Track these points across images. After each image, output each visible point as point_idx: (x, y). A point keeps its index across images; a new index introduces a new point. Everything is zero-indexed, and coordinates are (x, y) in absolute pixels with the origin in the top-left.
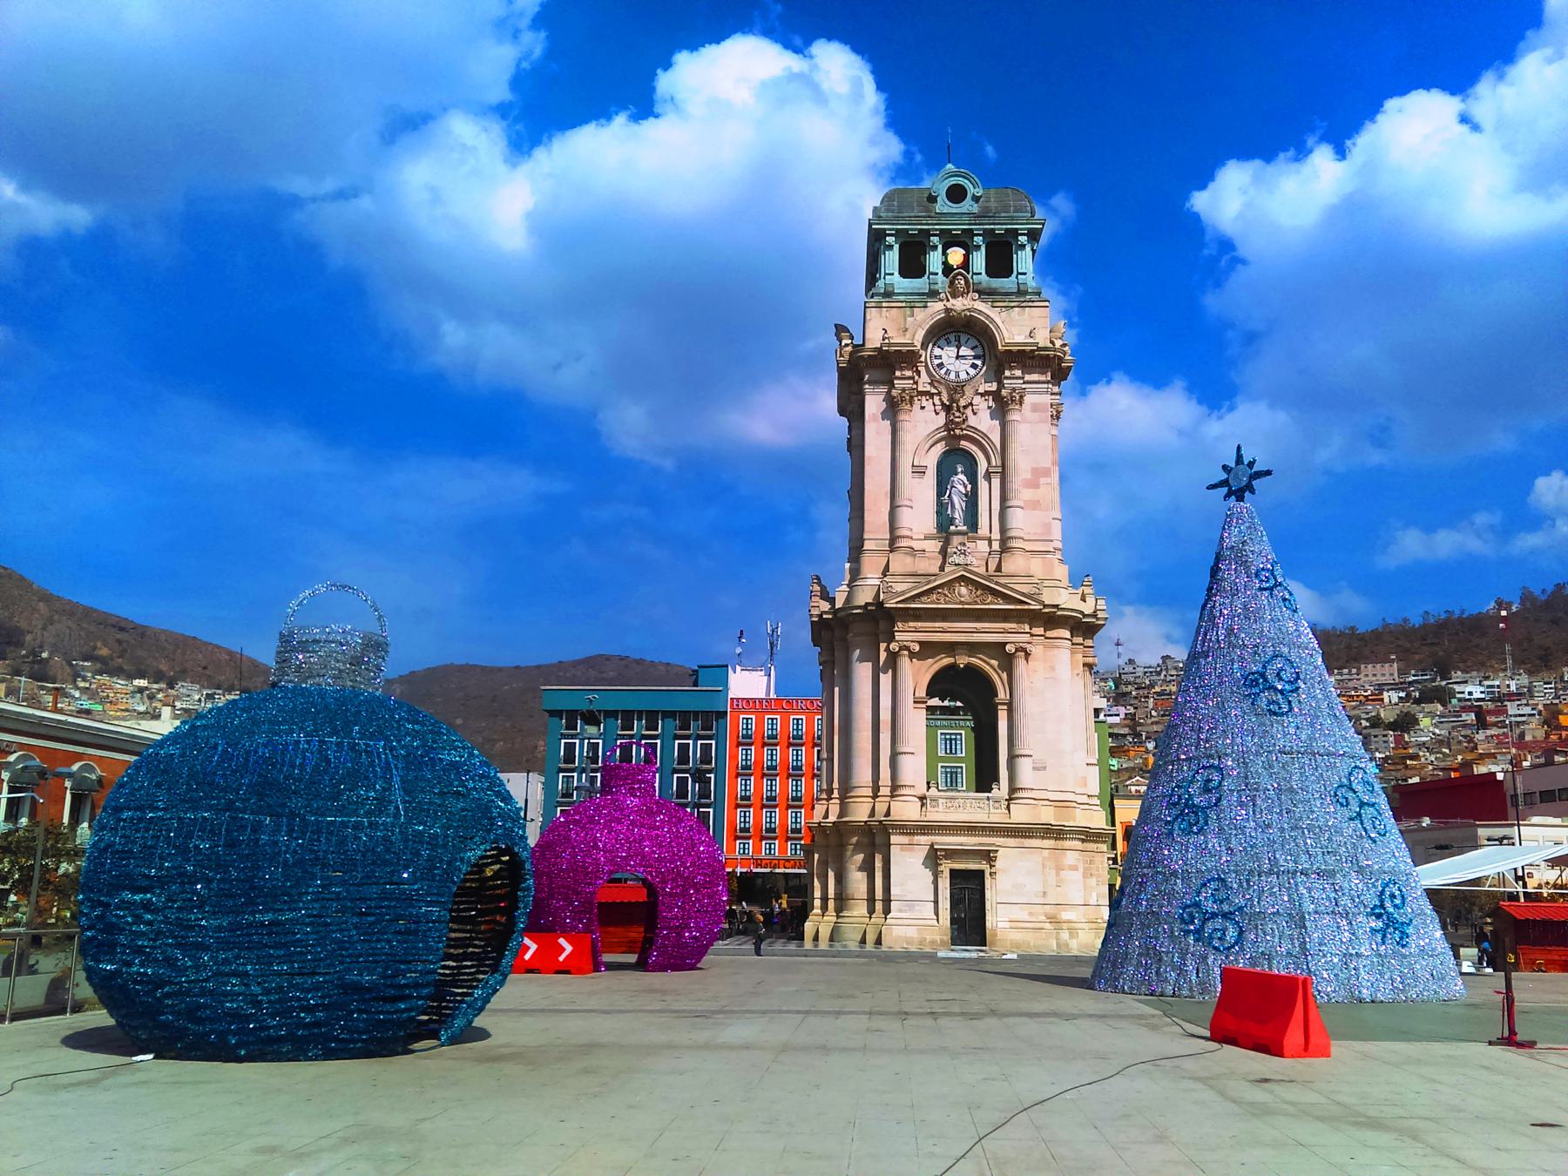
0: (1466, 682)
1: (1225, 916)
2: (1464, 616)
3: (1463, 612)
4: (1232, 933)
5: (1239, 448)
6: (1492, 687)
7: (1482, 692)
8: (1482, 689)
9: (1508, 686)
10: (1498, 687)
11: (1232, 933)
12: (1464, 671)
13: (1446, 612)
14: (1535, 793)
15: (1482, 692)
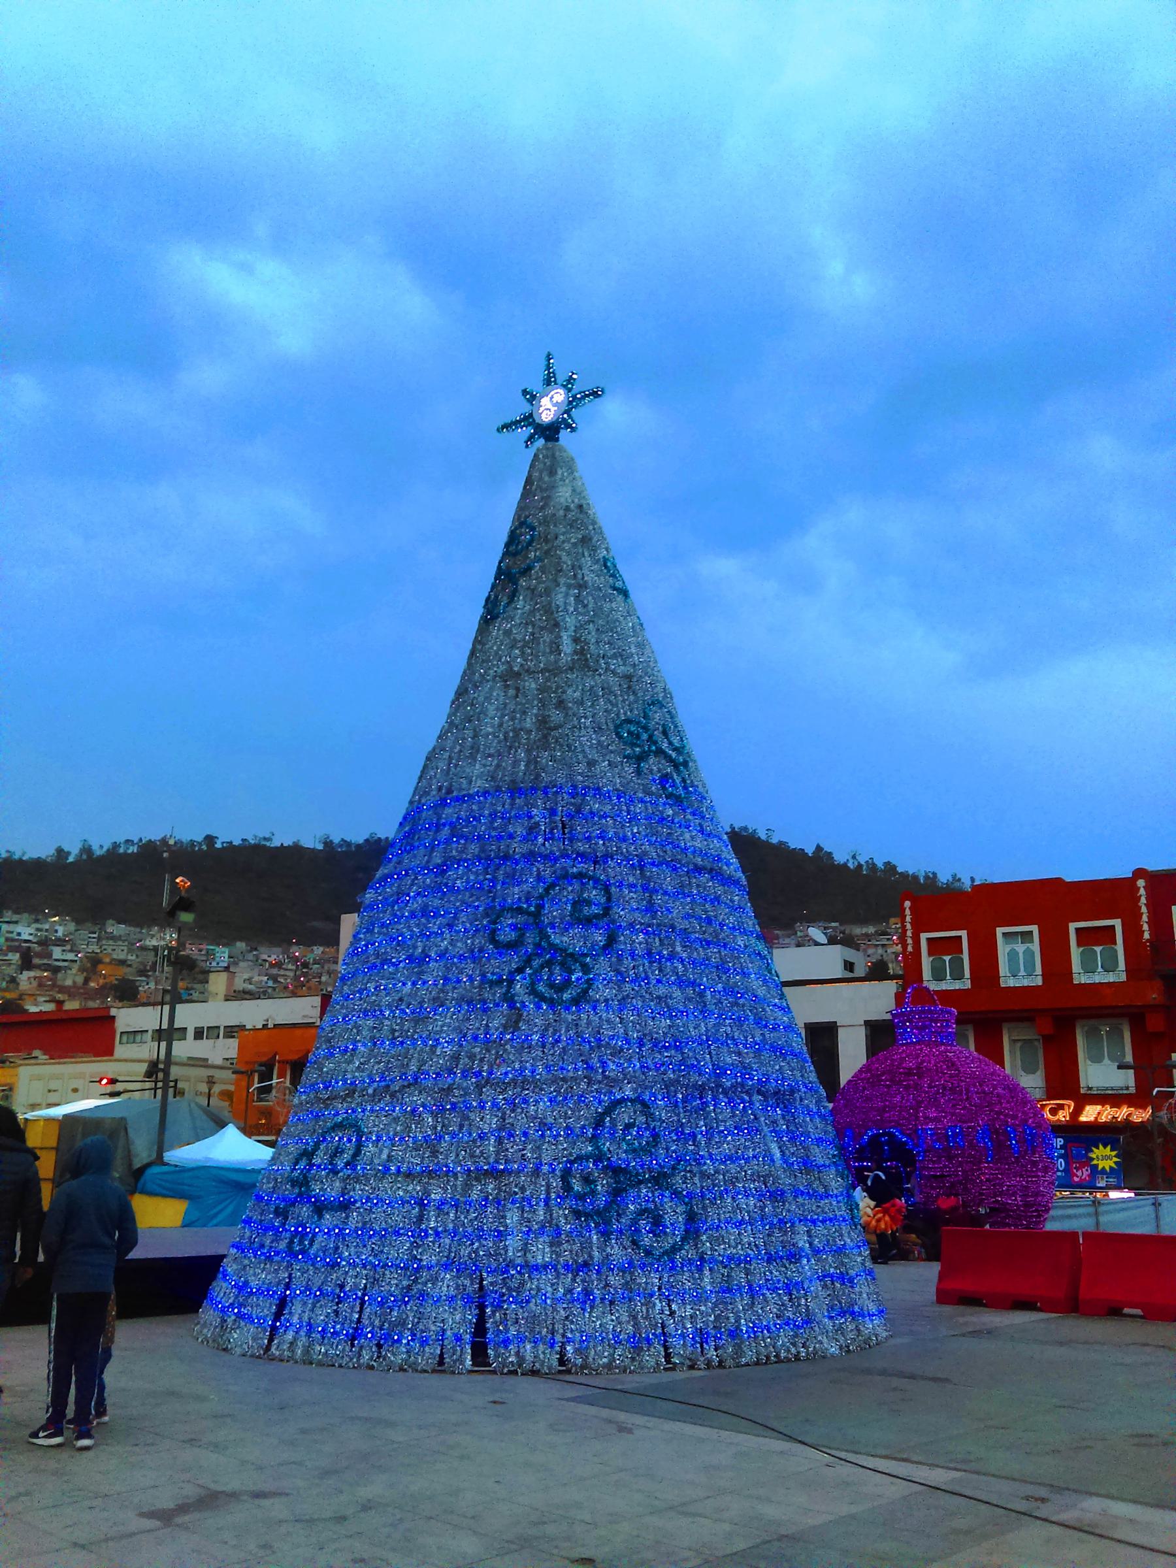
0: (16, 922)
1: (660, 1180)
2: (24, 858)
3: (24, 854)
4: (673, 1214)
5: (549, 357)
6: (38, 930)
7: (31, 934)
8: (32, 931)
9: (56, 931)
10: (47, 930)
11: (673, 1214)
12: (16, 912)
13: (8, 851)
14: (147, 1031)
15: (31, 934)
